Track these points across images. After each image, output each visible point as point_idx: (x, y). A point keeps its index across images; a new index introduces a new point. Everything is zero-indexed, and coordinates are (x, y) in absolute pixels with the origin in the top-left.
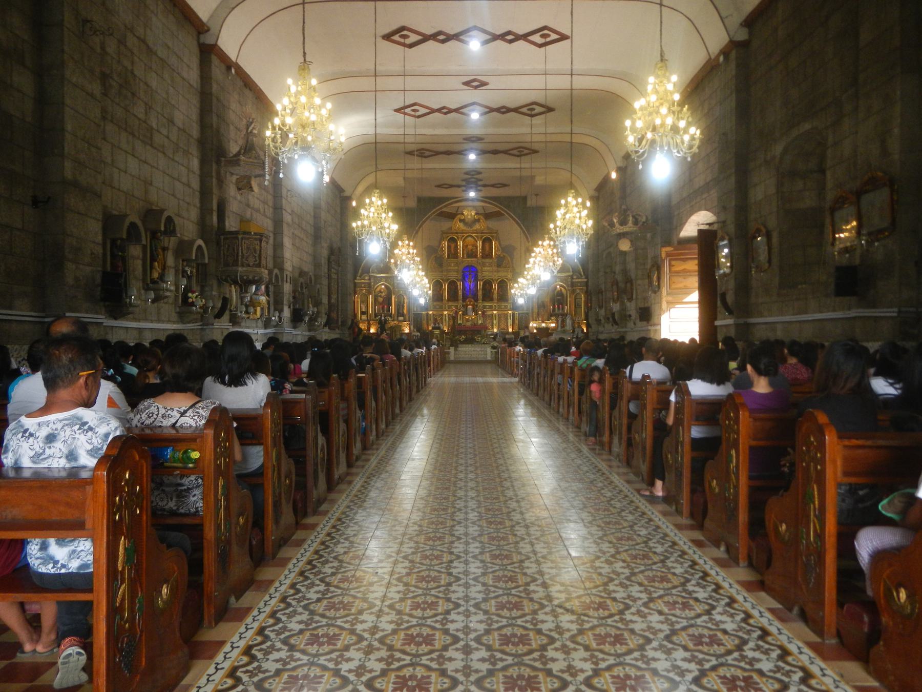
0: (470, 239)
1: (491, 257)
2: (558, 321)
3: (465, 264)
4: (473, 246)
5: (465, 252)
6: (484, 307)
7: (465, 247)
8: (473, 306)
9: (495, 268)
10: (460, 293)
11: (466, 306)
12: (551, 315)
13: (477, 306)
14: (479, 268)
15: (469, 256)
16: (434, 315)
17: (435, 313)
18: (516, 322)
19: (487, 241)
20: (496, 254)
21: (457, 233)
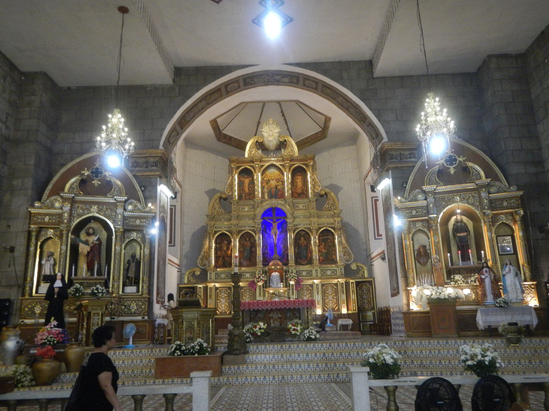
0: (273, 171)
1: (307, 197)
2: (482, 281)
3: (266, 205)
4: (278, 180)
5: (266, 190)
6: (299, 273)
7: (266, 182)
8: (281, 271)
9: (314, 211)
10: (259, 251)
11: (267, 274)
12: (450, 273)
13: (286, 272)
14: (287, 209)
15: (271, 196)
16: (217, 289)
17: (217, 285)
18: (353, 297)
19: (299, 172)
20: (313, 191)
21: (253, 162)
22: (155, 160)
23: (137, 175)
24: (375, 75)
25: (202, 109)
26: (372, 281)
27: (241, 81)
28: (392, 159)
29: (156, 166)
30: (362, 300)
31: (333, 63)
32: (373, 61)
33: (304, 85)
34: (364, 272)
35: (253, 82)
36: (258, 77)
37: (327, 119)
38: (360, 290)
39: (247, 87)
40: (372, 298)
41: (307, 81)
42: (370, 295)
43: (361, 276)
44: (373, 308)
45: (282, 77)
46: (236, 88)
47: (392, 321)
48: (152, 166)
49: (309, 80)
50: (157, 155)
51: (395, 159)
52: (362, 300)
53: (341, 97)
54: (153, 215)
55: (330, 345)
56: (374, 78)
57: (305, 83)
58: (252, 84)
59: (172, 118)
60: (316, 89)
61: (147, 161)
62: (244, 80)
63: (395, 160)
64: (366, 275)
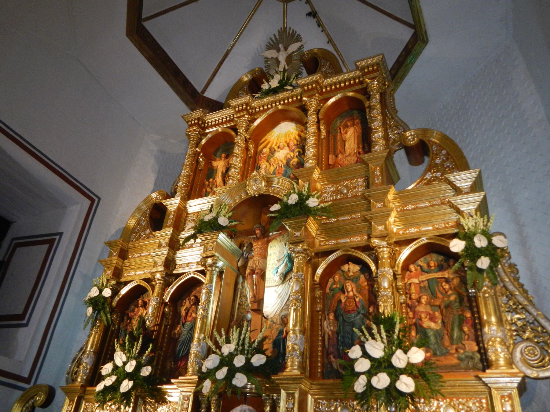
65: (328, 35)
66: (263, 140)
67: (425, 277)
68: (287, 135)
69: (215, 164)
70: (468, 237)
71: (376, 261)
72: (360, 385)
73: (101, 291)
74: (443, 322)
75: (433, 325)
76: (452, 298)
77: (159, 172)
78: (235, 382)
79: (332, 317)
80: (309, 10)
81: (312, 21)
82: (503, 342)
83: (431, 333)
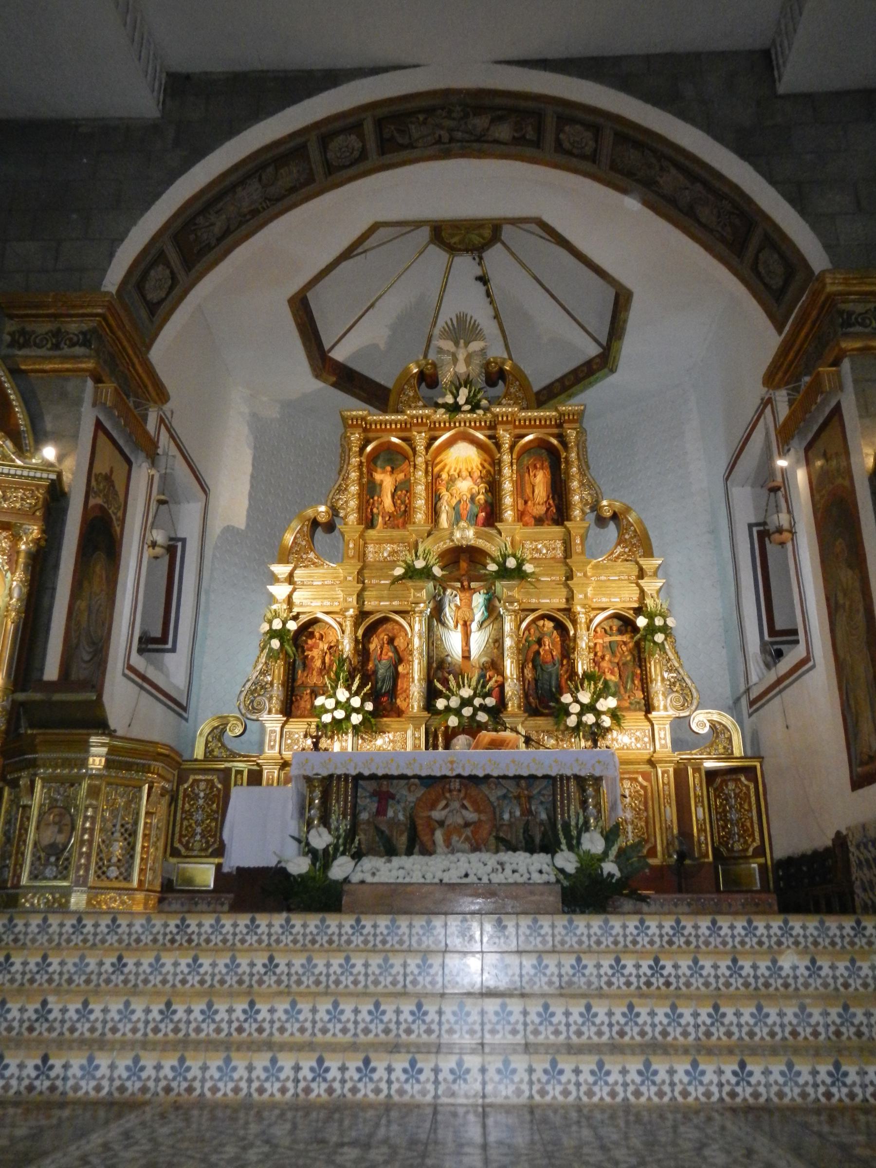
22: (85, 327)
23: (23, 367)
24: (781, 89)
25: (254, 213)
26: (755, 767)
27: (369, 127)
28: (850, 325)
29: (86, 343)
30: (724, 827)
31: (648, 58)
32: (773, 52)
33: (559, 147)
34: (730, 739)
35: (404, 141)
36: (421, 117)
37: (622, 300)
38: (717, 797)
39: (388, 159)
40: (755, 818)
41: (567, 128)
42: (750, 810)
43: (721, 751)
44: (760, 851)
45: (492, 121)
46: (356, 154)
47: (855, 873)
48: (73, 345)
49: (573, 121)
50: (88, 311)
51: (860, 324)
52: (724, 827)
53: (673, 171)
54: (53, 476)
55: (678, 928)
56: (782, 97)
57: (562, 136)
58: (403, 147)
59: (147, 208)
60: (593, 158)
61: (59, 331)
62: (379, 123)
63: (858, 329)
64: (738, 751)
65: (496, 310)
66: (438, 460)
67: (608, 639)
68: (467, 460)
69: (378, 477)
70: (651, 617)
71: (574, 622)
72: (572, 721)
73: (284, 623)
74: (620, 676)
75: (613, 678)
76: (629, 658)
77: (255, 448)
78: (478, 718)
79: (530, 665)
80: (479, 272)
81: (480, 288)
82: (663, 694)
83: (611, 684)
